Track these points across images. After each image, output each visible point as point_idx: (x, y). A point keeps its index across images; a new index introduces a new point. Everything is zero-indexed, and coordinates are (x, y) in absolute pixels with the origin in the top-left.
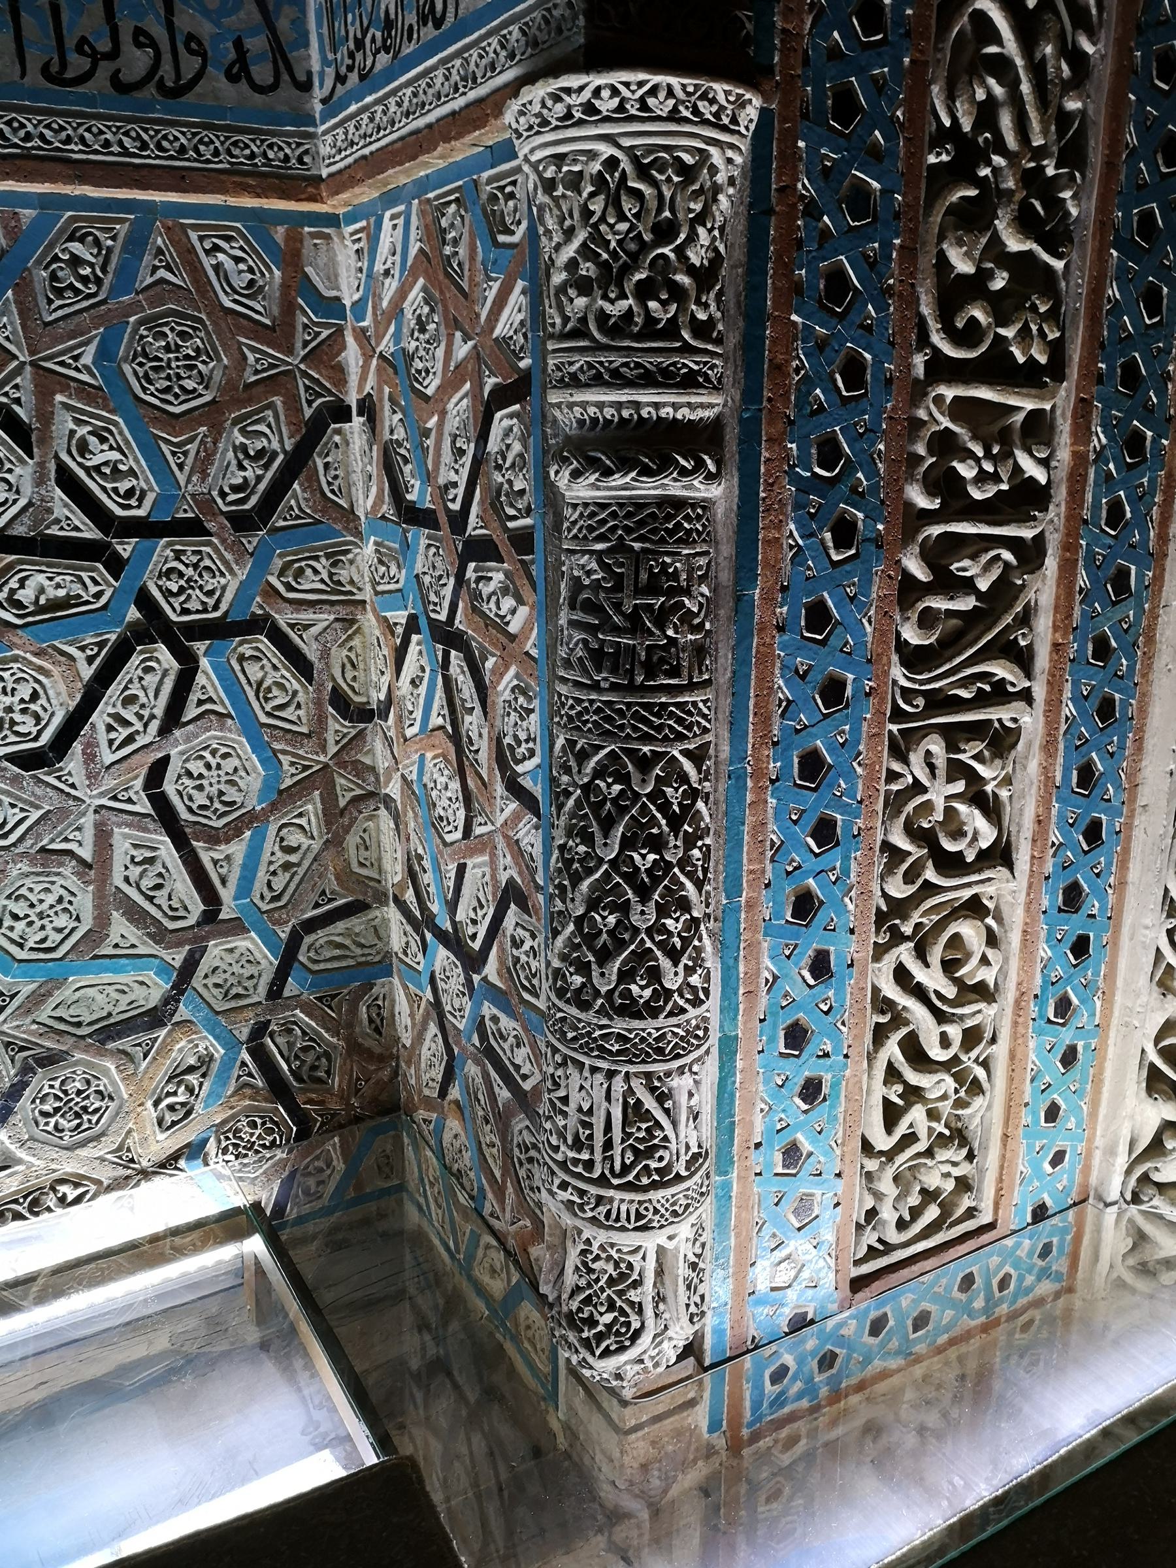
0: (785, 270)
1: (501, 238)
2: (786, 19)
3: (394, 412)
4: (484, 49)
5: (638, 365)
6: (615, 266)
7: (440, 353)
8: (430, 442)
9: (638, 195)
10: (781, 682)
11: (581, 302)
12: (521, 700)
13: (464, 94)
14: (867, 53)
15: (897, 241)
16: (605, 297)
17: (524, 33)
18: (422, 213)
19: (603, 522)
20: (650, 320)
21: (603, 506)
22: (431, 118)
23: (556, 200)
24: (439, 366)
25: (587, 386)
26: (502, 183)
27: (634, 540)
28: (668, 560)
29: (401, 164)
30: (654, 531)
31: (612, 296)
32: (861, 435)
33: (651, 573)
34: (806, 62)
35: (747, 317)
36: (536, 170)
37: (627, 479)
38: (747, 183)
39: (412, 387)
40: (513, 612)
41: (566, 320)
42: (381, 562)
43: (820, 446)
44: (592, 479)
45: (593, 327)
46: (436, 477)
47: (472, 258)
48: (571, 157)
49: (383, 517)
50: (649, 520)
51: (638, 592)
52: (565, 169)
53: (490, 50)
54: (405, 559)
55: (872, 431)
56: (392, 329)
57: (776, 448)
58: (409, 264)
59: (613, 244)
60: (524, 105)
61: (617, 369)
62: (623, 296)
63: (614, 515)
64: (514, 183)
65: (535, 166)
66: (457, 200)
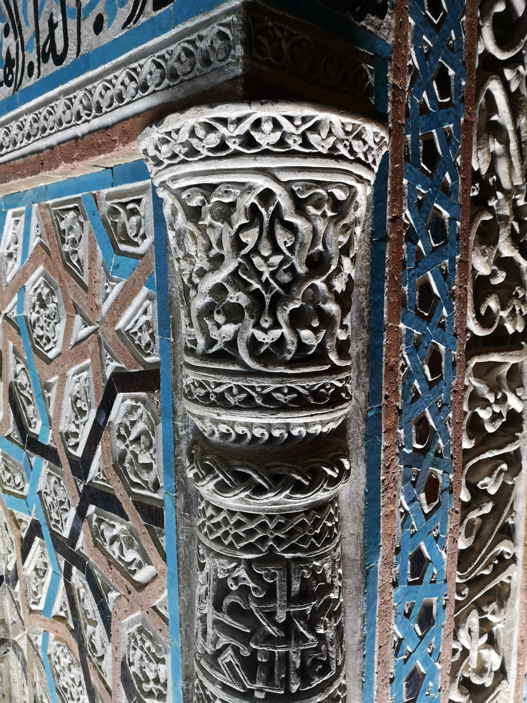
0: (396, 286)
1: (123, 247)
2: (395, 77)
3: (18, 362)
4: (110, 82)
5: (292, 390)
6: (268, 298)
7: (61, 328)
8: (52, 394)
9: (291, 228)
10: (395, 627)
11: (229, 329)
12: (148, 644)
13: (87, 121)
14: (442, 111)
15: (458, 257)
16: (257, 325)
17: (159, 66)
18: (42, 216)
19: (251, 533)
20: (302, 346)
21: (251, 517)
22: (52, 140)
23: (203, 229)
24: (60, 338)
25: (236, 408)
26: (124, 200)
27: (285, 551)
28: (317, 564)
29: (23, 176)
30: (303, 540)
31: (266, 325)
32: (440, 409)
33: (303, 580)
34: (407, 114)
35: (370, 330)
36: (178, 198)
37: (281, 497)
38: (370, 214)
39: (34, 347)
40: (140, 566)
41: (211, 342)
42: (7, 469)
43: (417, 425)
44: (243, 495)
45: (243, 353)
46: (58, 424)
47: (92, 259)
48: (223, 188)
49: (9, 437)
50: (300, 530)
51: (291, 600)
52: (214, 200)
53: (117, 83)
54: (28, 476)
55: (446, 404)
56: (15, 299)
57: (391, 436)
58: (30, 251)
59: (266, 275)
60: (169, 133)
61: (269, 394)
62: (276, 325)
63: (263, 526)
64: (138, 201)
65: (177, 194)
66: (75, 209)
